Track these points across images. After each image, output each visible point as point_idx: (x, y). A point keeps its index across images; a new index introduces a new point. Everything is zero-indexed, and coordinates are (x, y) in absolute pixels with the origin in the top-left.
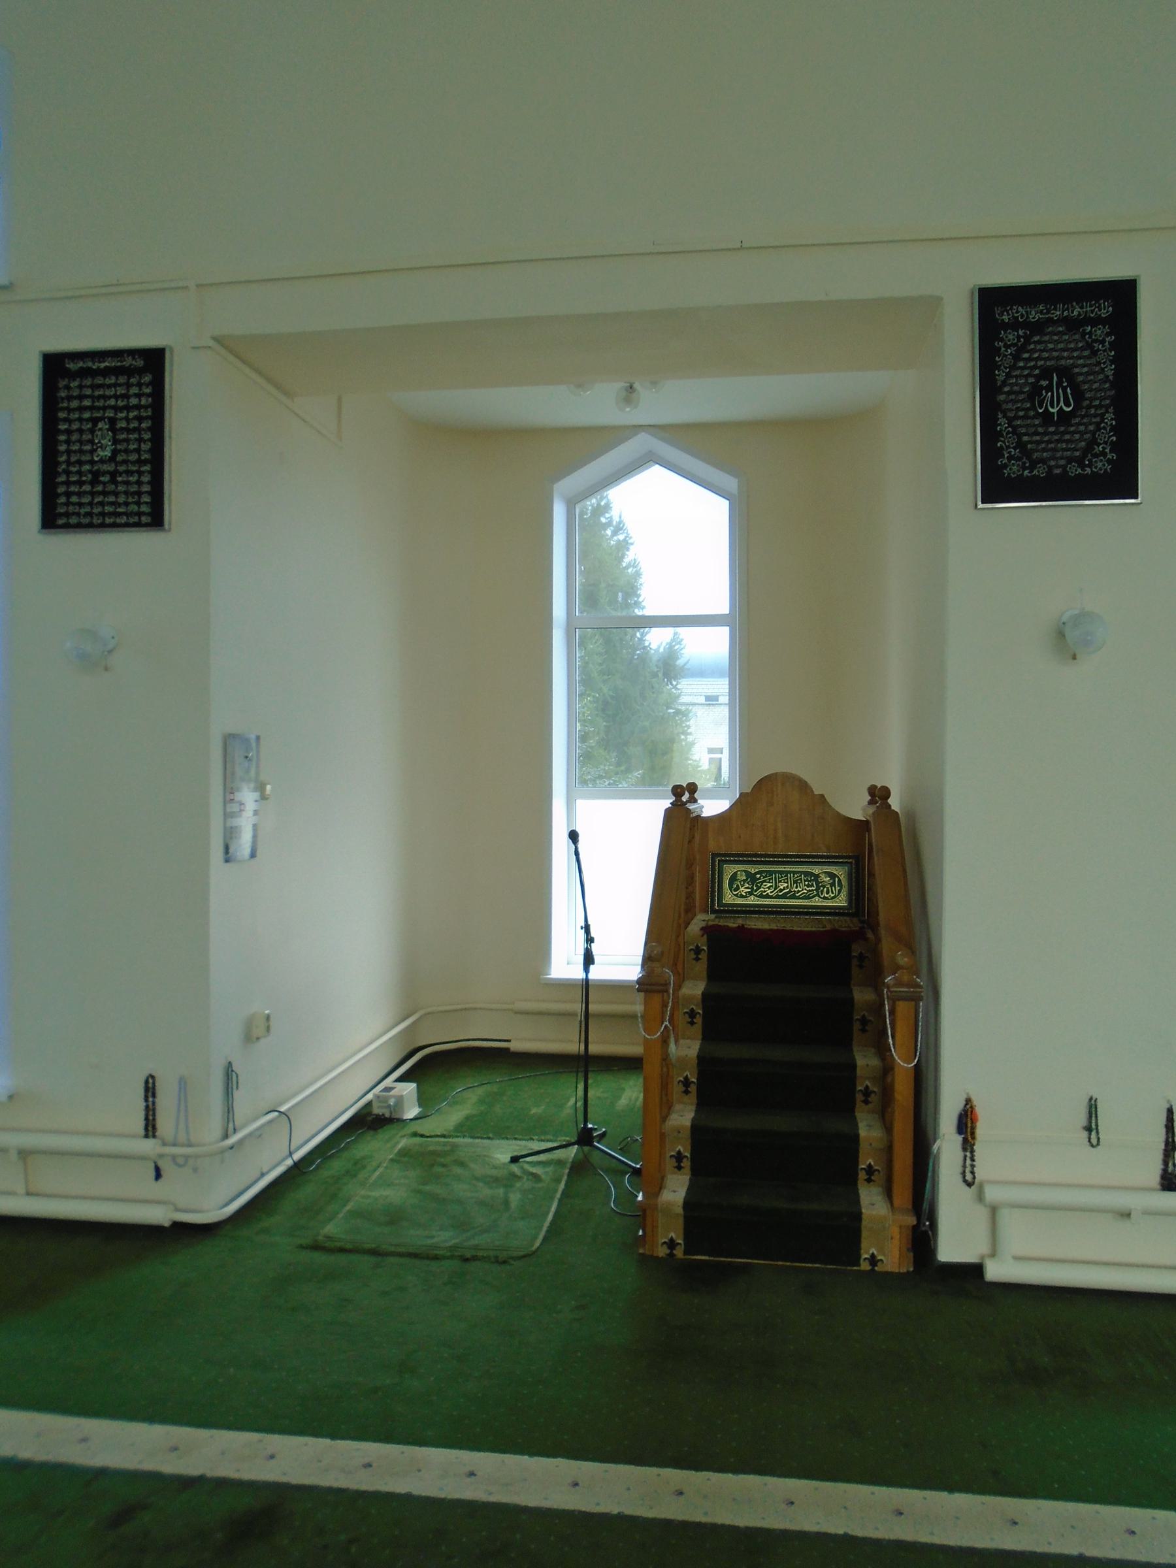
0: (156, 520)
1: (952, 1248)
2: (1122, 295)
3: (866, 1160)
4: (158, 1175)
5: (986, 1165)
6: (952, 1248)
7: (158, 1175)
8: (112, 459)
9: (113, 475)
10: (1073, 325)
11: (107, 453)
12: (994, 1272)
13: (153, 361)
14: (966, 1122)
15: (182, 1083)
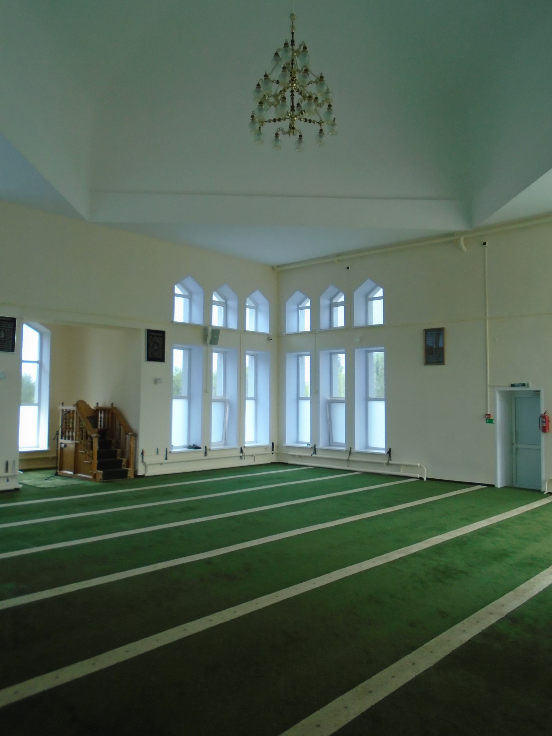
0: (13, 350)
1: (140, 473)
2: (163, 333)
3: (124, 463)
4: (8, 481)
5: (145, 460)
6: (140, 473)
7: (8, 481)
8: (4, 337)
9: (4, 341)
10: (158, 336)
11: (3, 336)
12: (148, 474)
13: (13, 320)
14: (142, 453)
15: (14, 462)
